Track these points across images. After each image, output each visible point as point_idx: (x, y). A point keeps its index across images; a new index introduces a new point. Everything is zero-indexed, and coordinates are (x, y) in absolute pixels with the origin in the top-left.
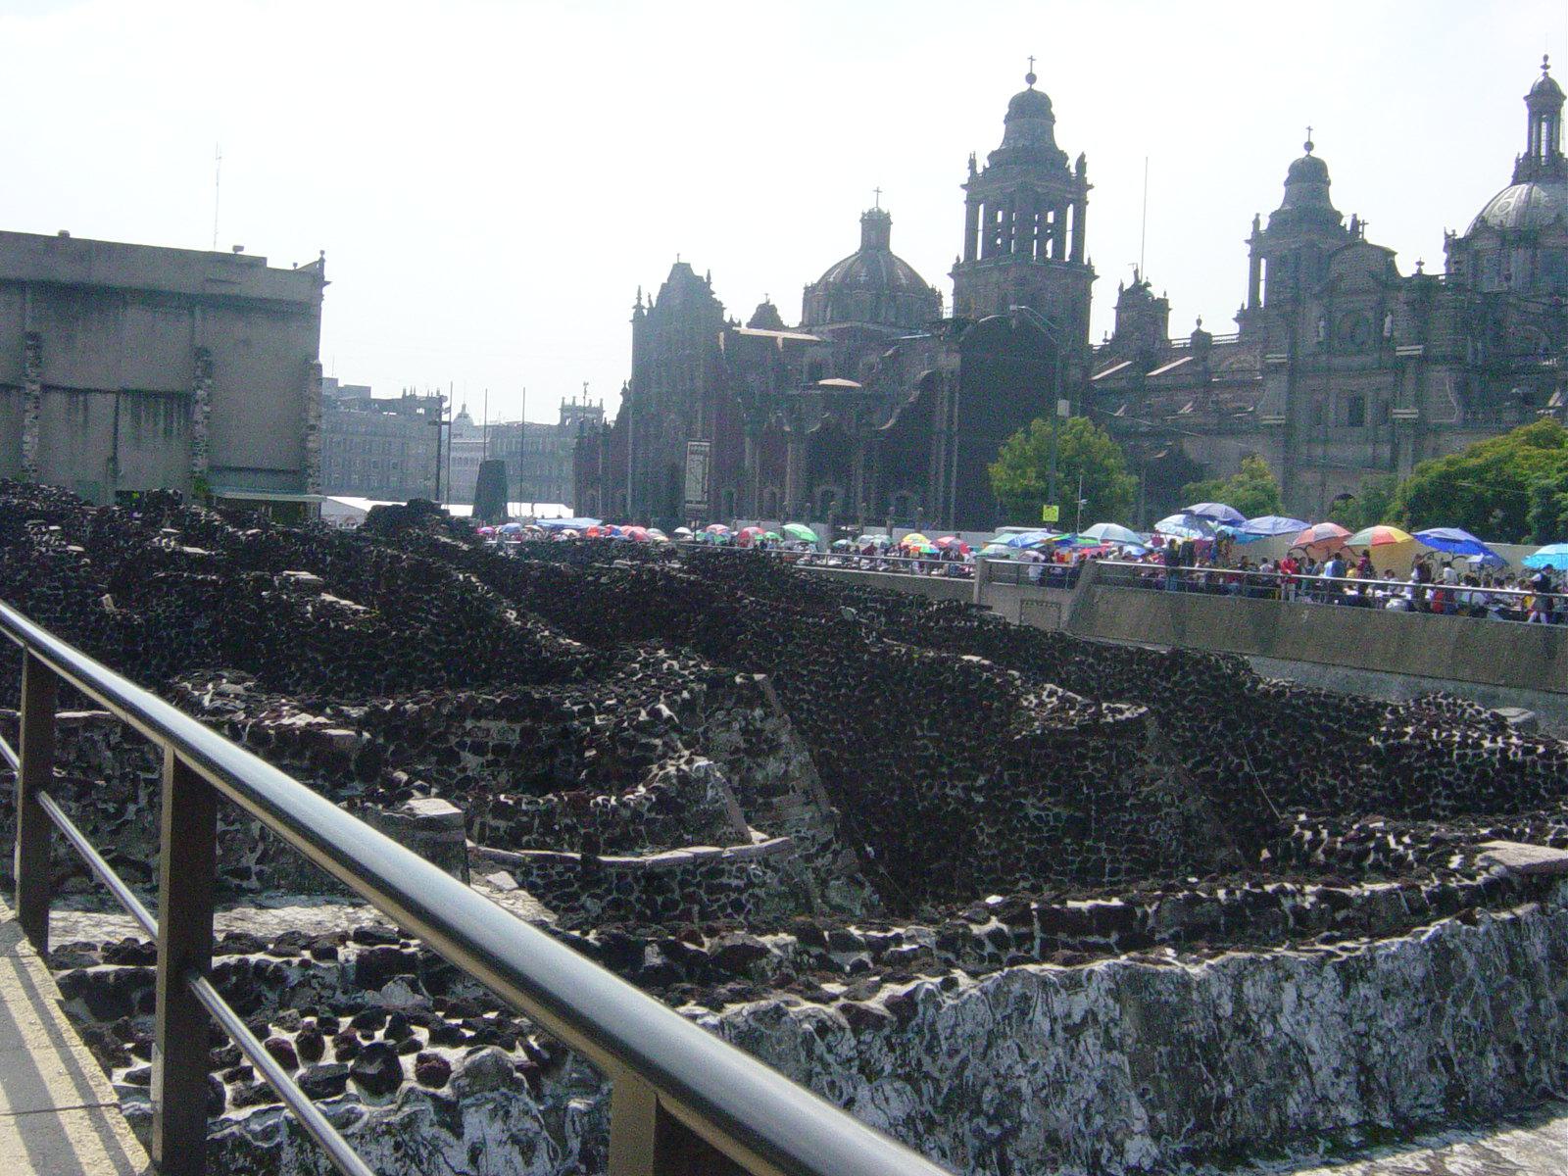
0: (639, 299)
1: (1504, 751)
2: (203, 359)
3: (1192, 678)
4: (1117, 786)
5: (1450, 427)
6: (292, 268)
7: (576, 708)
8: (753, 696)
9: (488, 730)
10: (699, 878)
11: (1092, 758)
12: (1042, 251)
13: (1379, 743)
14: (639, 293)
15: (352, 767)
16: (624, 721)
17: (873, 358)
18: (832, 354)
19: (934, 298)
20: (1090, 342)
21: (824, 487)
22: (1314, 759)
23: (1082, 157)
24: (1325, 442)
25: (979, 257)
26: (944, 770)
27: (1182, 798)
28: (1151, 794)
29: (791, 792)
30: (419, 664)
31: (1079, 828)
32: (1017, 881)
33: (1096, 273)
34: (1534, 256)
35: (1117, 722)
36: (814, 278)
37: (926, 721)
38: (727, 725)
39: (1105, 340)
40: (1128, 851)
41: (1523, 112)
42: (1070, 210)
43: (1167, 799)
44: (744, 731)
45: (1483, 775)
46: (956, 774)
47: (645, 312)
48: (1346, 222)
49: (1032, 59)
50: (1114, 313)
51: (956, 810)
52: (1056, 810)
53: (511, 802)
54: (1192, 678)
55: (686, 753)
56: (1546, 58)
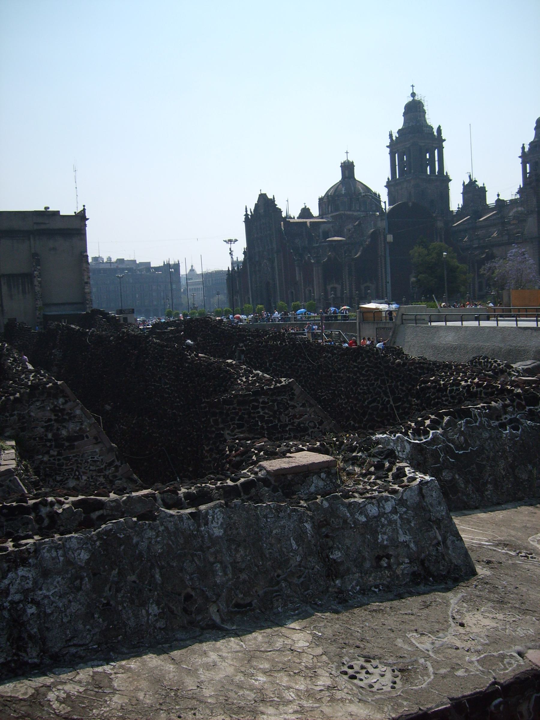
0: (246, 211)
2: (36, 259)
3: (366, 360)
4: (279, 421)
6: (74, 214)
14: (246, 209)
17: (350, 226)
18: (332, 227)
19: (376, 198)
20: (451, 209)
21: (332, 286)
23: (439, 127)
25: (398, 177)
28: (299, 424)
29: (86, 439)
33: (451, 178)
38: (42, 408)
39: (459, 208)
42: (436, 151)
43: (312, 424)
47: (249, 216)
49: (413, 86)
50: (461, 196)
54: (366, 360)
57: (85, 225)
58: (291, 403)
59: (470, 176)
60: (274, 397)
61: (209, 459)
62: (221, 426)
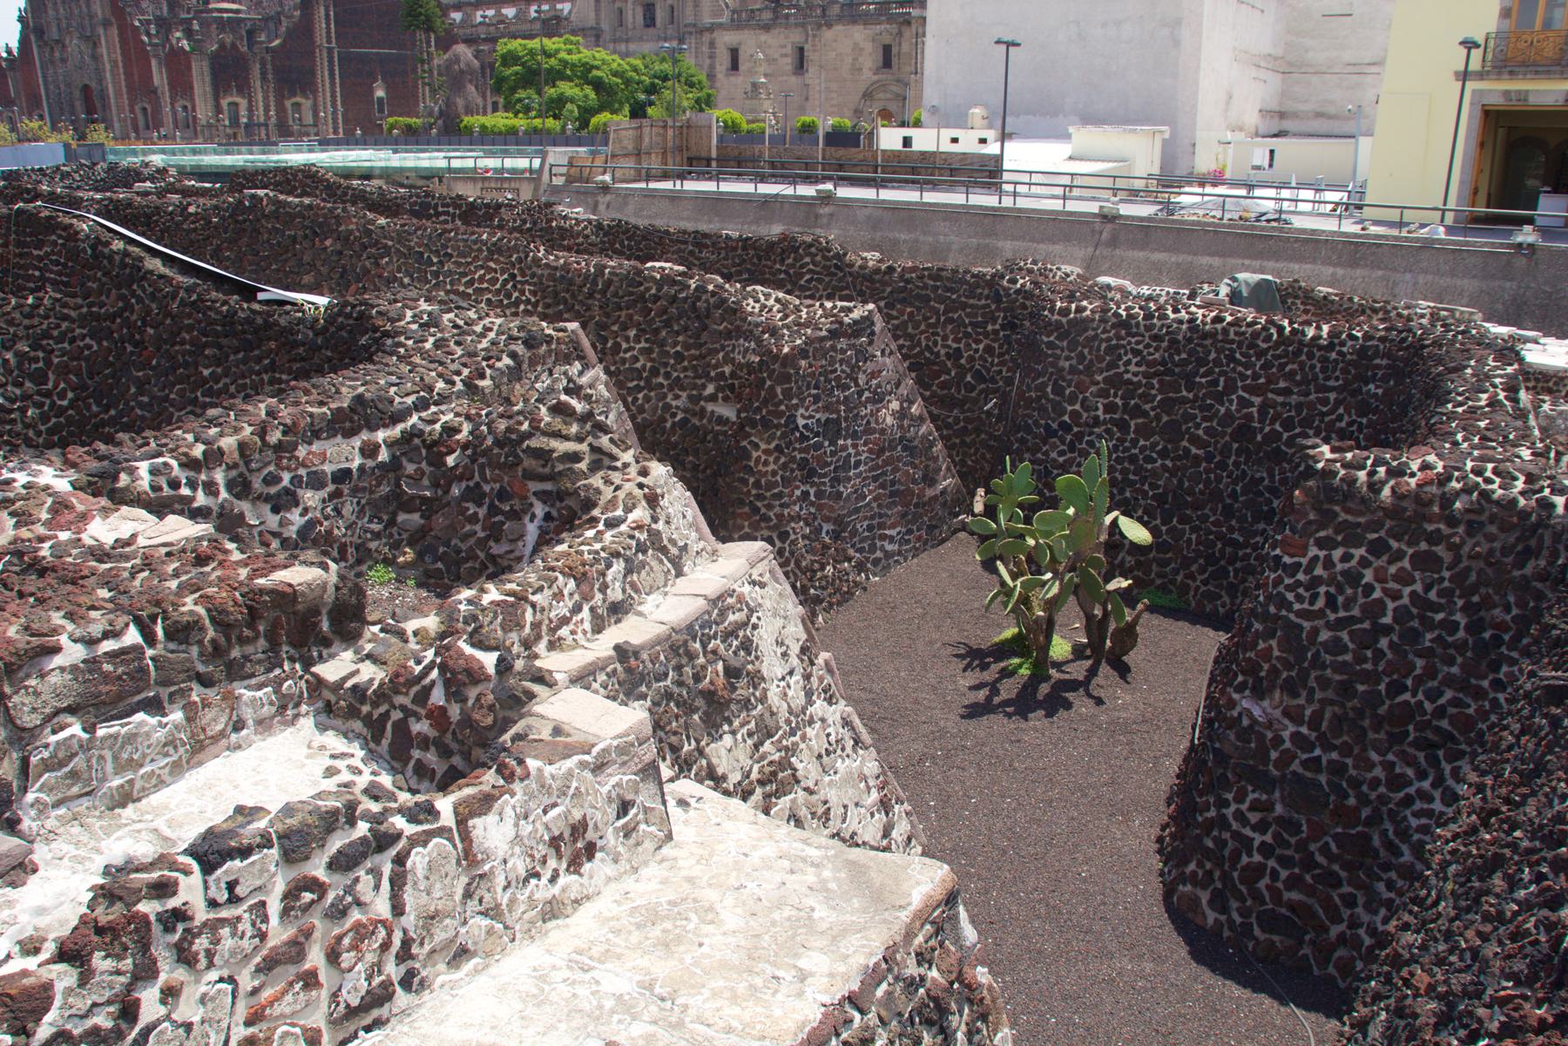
1: (1192, 321)
5: (721, 26)
8: (572, 352)
9: (324, 454)
15: (325, 626)
21: (230, 99)
22: (935, 326)
24: (627, 41)
26: (661, 380)
27: (898, 385)
28: (879, 386)
30: (56, 333)
37: (632, 333)
40: (865, 444)
45: (1173, 342)
46: (677, 384)
51: (685, 421)
54: (807, 259)
61: (772, 467)
62: (795, 401)
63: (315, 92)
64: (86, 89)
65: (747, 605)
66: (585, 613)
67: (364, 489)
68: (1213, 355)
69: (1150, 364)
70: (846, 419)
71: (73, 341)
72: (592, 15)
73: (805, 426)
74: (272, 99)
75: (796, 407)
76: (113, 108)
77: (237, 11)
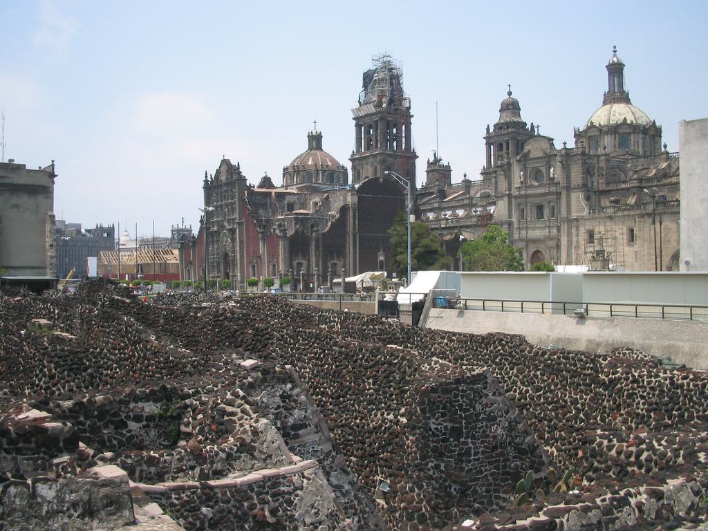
0: (206, 177)
1: (671, 379)
3: (500, 348)
4: (475, 410)
5: (583, 218)
7: (191, 392)
10: (267, 489)
11: (461, 396)
12: (391, 146)
13: (604, 377)
14: (206, 173)
15: (61, 445)
16: (218, 399)
17: (317, 199)
18: (298, 199)
21: (298, 261)
27: (507, 412)
30: (105, 366)
31: (456, 433)
32: (428, 463)
34: (615, 138)
35: (473, 376)
36: (288, 163)
37: (371, 381)
39: (423, 186)
40: (483, 442)
41: (606, 73)
42: (404, 127)
43: (500, 413)
44: (281, 396)
45: (662, 391)
46: (389, 409)
48: (529, 126)
52: (445, 424)
53: (157, 455)
55: (254, 416)
56: (615, 47)
57: (53, 182)
58: (484, 391)
59: (435, 155)
60: (471, 386)
63: (345, 257)
64: (226, 255)
65: (294, 484)
66: (197, 470)
67: (161, 426)
68: (681, 398)
69: (650, 404)
70: (466, 428)
71: (111, 370)
72: (507, 212)
73: (436, 429)
74: (321, 261)
75: (429, 418)
76: (238, 265)
77: (307, 214)
